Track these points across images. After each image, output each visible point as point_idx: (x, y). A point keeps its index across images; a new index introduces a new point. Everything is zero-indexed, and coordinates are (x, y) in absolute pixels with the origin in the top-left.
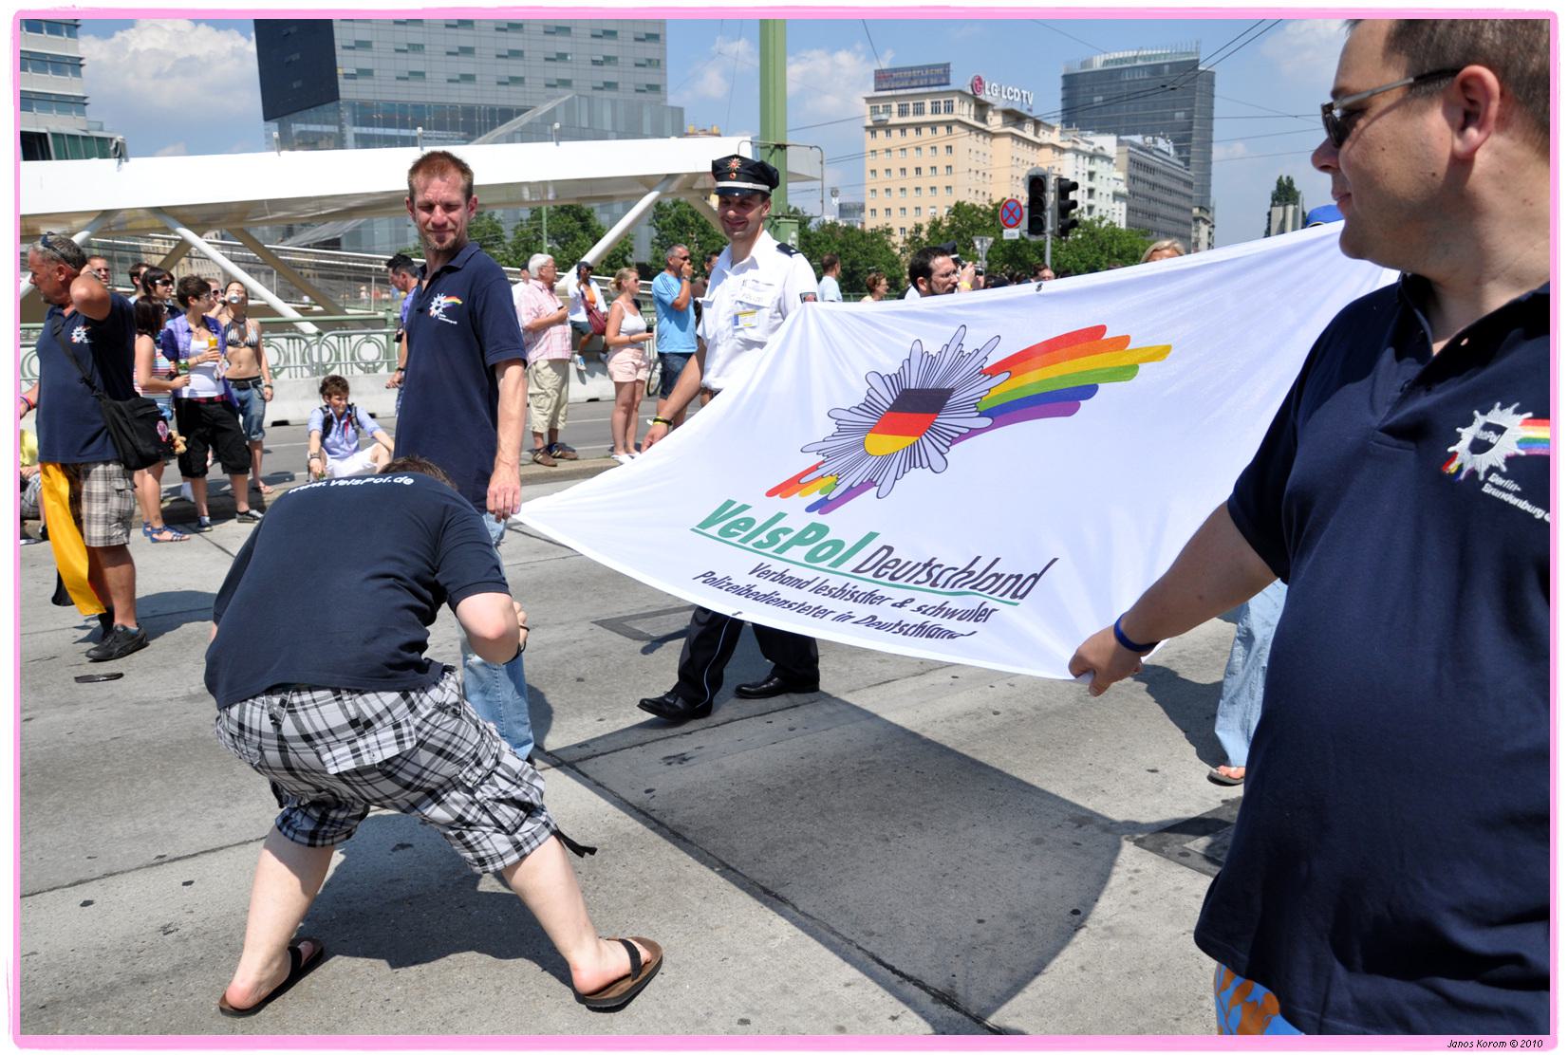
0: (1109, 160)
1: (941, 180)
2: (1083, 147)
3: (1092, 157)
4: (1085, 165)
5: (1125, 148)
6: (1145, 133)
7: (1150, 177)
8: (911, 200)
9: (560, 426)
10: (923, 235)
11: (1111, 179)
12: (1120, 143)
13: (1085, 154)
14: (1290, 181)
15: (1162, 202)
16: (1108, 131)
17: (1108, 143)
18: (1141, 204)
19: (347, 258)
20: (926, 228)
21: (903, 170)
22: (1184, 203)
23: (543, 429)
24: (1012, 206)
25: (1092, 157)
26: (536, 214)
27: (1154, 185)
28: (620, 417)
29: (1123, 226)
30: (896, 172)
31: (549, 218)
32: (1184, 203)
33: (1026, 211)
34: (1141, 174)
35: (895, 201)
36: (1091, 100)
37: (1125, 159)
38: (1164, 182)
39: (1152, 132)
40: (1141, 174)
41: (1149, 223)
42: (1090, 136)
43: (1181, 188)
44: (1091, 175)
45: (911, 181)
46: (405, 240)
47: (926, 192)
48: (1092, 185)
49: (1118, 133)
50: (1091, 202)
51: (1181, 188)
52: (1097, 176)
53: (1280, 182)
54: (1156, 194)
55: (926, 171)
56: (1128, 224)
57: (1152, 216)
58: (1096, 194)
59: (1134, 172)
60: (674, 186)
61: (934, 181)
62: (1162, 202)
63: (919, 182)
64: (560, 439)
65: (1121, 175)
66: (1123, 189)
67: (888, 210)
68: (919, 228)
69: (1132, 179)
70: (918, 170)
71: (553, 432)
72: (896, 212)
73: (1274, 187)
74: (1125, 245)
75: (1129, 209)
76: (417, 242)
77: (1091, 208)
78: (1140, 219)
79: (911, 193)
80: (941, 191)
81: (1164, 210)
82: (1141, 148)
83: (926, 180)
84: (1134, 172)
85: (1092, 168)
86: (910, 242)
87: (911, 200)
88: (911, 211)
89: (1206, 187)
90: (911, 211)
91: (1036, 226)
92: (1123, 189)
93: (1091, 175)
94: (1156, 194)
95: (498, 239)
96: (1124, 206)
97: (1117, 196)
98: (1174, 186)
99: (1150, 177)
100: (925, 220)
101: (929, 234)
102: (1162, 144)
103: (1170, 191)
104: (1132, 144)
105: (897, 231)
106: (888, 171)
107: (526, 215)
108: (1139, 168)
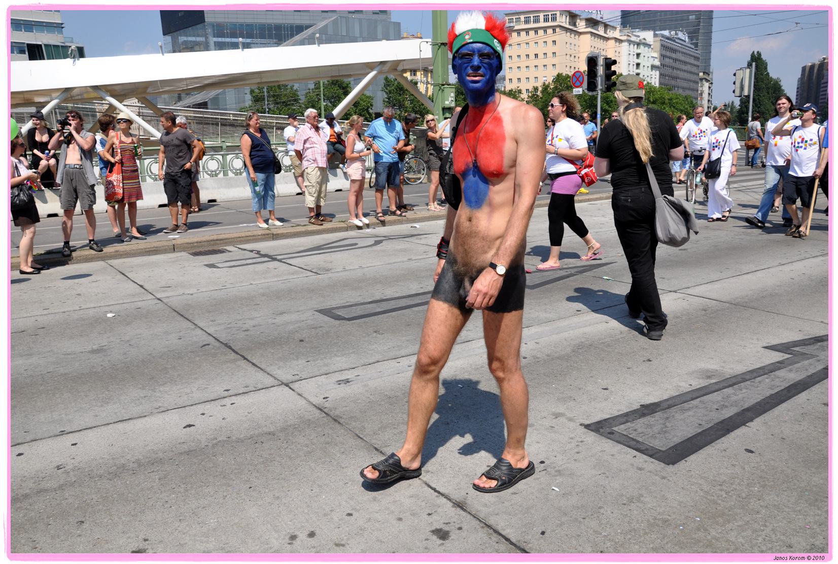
1: (550, 60)
7: (674, 55)
8: (532, 73)
9: (322, 203)
10: (539, 93)
11: (651, 57)
18: (669, 71)
19: (212, 113)
20: (540, 89)
21: (528, 56)
22: (694, 69)
23: (312, 205)
24: (577, 75)
26: (317, 85)
27: (675, 60)
28: (352, 199)
29: (657, 85)
30: (523, 57)
31: (325, 88)
32: (694, 69)
33: (586, 78)
34: (668, 54)
35: (523, 74)
38: (683, 58)
40: (668, 54)
41: (673, 82)
45: (532, 62)
46: (244, 101)
47: (541, 68)
48: (638, 61)
50: (638, 71)
52: (642, 55)
54: (677, 65)
55: (541, 56)
56: (660, 83)
58: (641, 66)
59: (664, 52)
60: (386, 68)
61: (545, 62)
63: (536, 62)
64: (323, 212)
65: (656, 55)
67: (519, 79)
68: (536, 89)
69: (663, 56)
70: (536, 55)
71: (318, 207)
72: (523, 80)
75: (661, 75)
76: (250, 103)
78: (667, 80)
79: (524, 69)
80: (550, 67)
83: (540, 62)
84: (664, 52)
85: (639, 51)
86: (531, 97)
87: (532, 73)
88: (532, 80)
89: (707, 60)
90: (532, 80)
91: (592, 86)
93: (638, 55)
94: (677, 65)
95: (296, 100)
96: (658, 73)
97: (653, 67)
98: (687, 60)
99: (674, 55)
100: (539, 84)
101: (542, 92)
103: (685, 63)
105: (524, 91)
106: (519, 56)
107: (312, 86)
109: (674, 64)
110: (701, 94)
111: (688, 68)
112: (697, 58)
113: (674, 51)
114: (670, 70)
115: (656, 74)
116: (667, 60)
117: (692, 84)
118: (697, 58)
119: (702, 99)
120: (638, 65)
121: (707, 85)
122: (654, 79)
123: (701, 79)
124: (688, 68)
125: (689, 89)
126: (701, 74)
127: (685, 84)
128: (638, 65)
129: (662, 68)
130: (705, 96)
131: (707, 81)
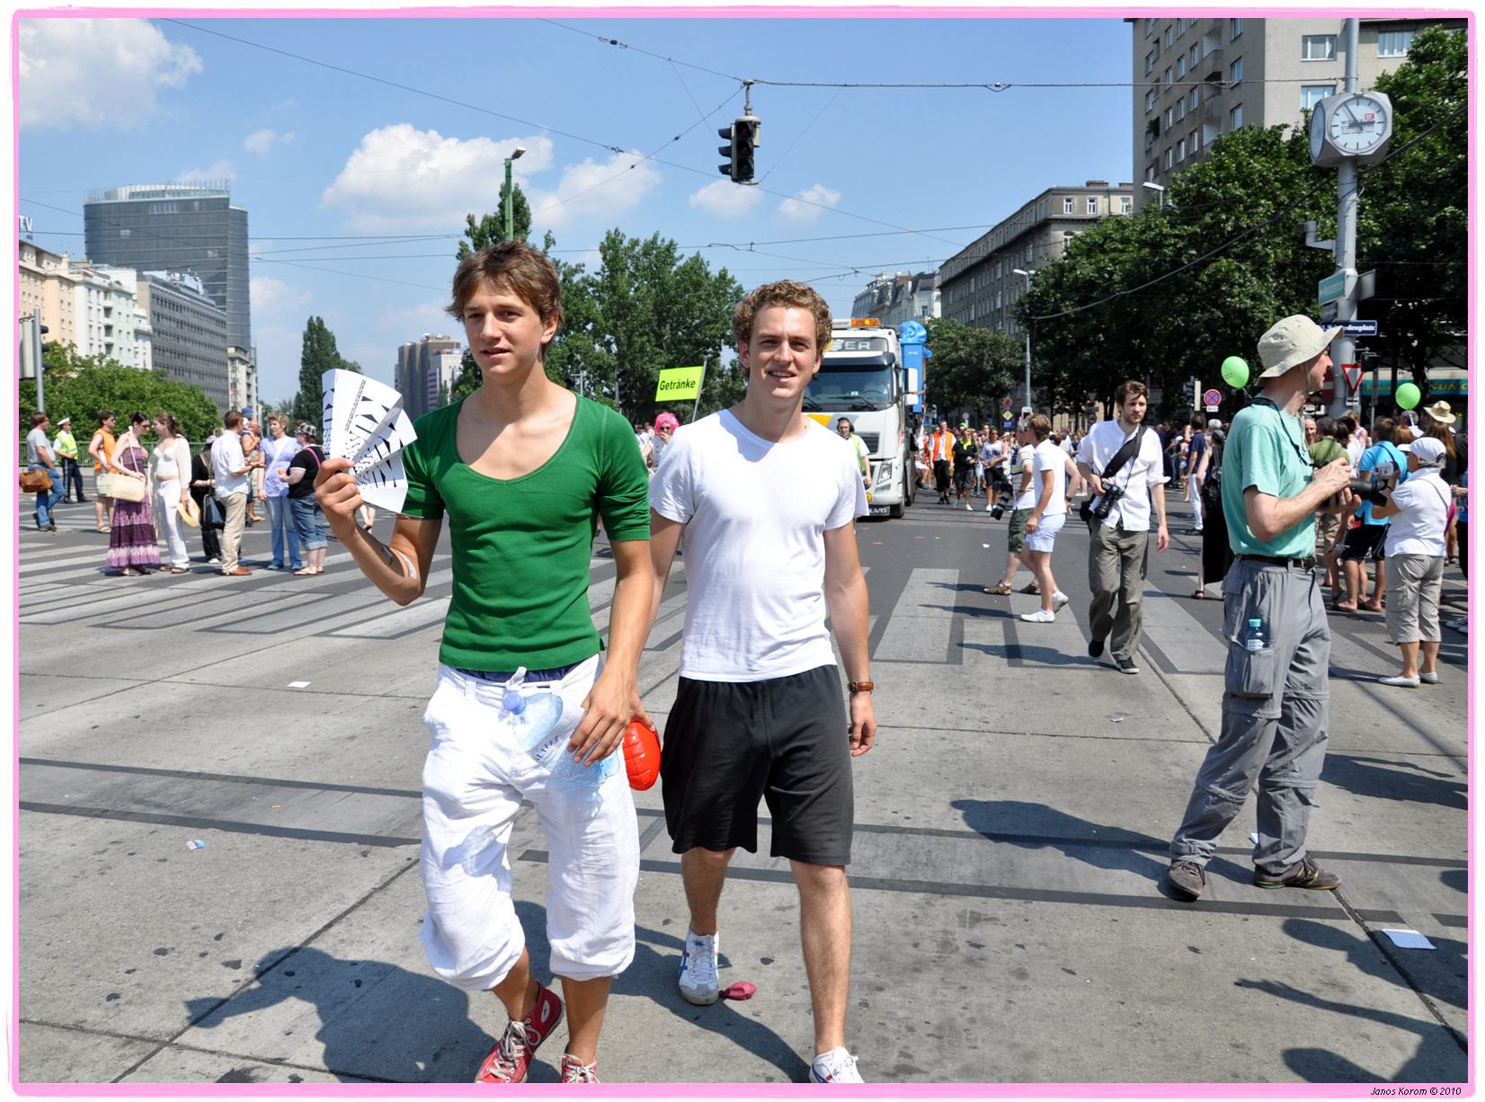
0: (128, 295)
2: (97, 280)
3: (107, 291)
4: (101, 301)
5: (146, 284)
6: (170, 270)
7: (177, 315)
11: (134, 314)
12: (140, 278)
13: (99, 288)
14: (320, 321)
15: (193, 341)
16: (128, 266)
17: (126, 278)
18: (169, 342)
22: (217, 341)
25: (107, 291)
27: (181, 323)
29: (149, 367)
32: (217, 341)
34: (166, 311)
36: (112, 233)
37: (146, 295)
38: (194, 321)
39: (182, 269)
40: (166, 311)
41: (179, 363)
42: (106, 270)
43: (213, 327)
44: (108, 311)
49: (139, 271)
50: (109, 340)
51: (213, 327)
52: (114, 313)
53: (310, 323)
54: (185, 332)
56: (155, 364)
57: (184, 355)
58: (115, 331)
59: (158, 309)
62: (193, 341)
65: (143, 312)
66: (146, 326)
69: (156, 316)
73: (305, 328)
74: (130, 385)
75: (154, 348)
77: (109, 346)
81: (194, 349)
82: (165, 284)
84: (158, 309)
85: (108, 303)
92: (146, 326)
93: (108, 311)
94: (185, 332)
96: (148, 345)
97: (139, 334)
98: (204, 324)
99: (177, 315)
102: (189, 281)
103: (200, 329)
104: (155, 280)
108: (162, 304)
109: (179, 331)
110: (234, 385)
111: (206, 338)
112: (223, 323)
113: (179, 308)
114: (174, 341)
115: (146, 347)
116: (165, 322)
117: (215, 366)
118: (222, 323)
119: (236, 393)
120: (108, 328)
121: (242, 369)
122: (137, 356)
123: (233, 359)
124: (206, 338)
125: (211, 375)
126: (231, 351)
127: (203, 367)
128: (108, 328)
129: (157, 336)
130: (242, 387)
131: (243, 362)
